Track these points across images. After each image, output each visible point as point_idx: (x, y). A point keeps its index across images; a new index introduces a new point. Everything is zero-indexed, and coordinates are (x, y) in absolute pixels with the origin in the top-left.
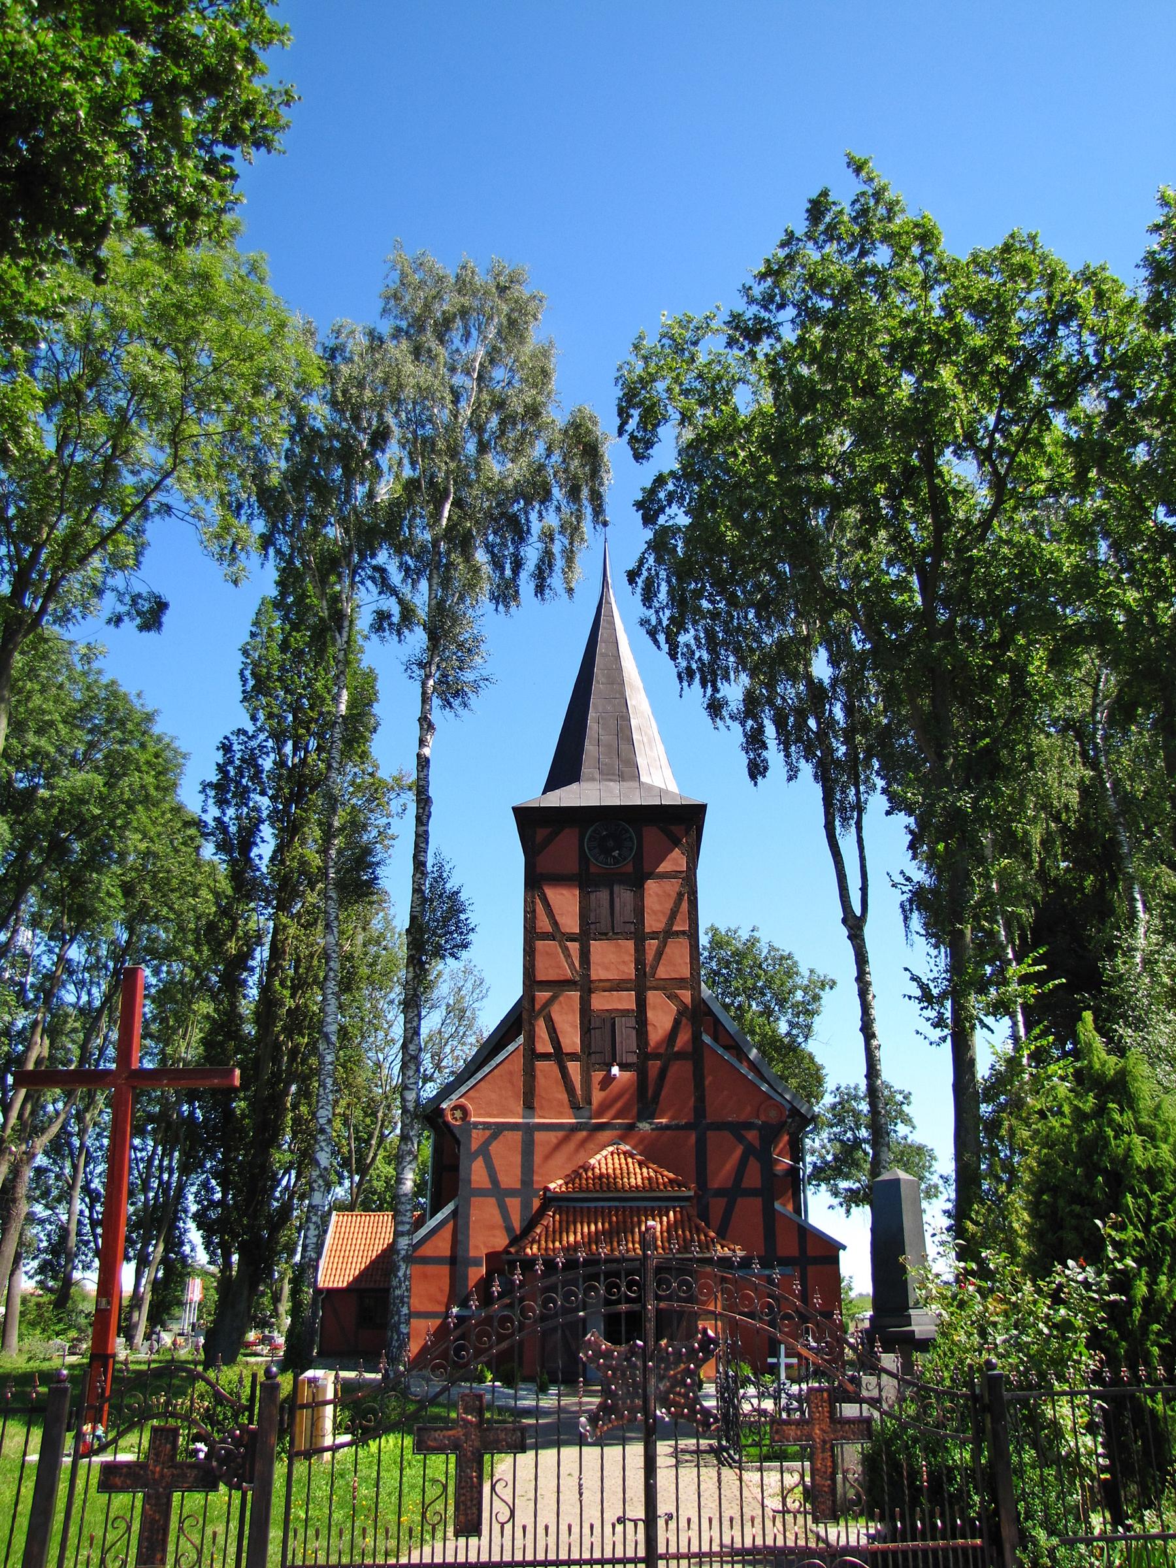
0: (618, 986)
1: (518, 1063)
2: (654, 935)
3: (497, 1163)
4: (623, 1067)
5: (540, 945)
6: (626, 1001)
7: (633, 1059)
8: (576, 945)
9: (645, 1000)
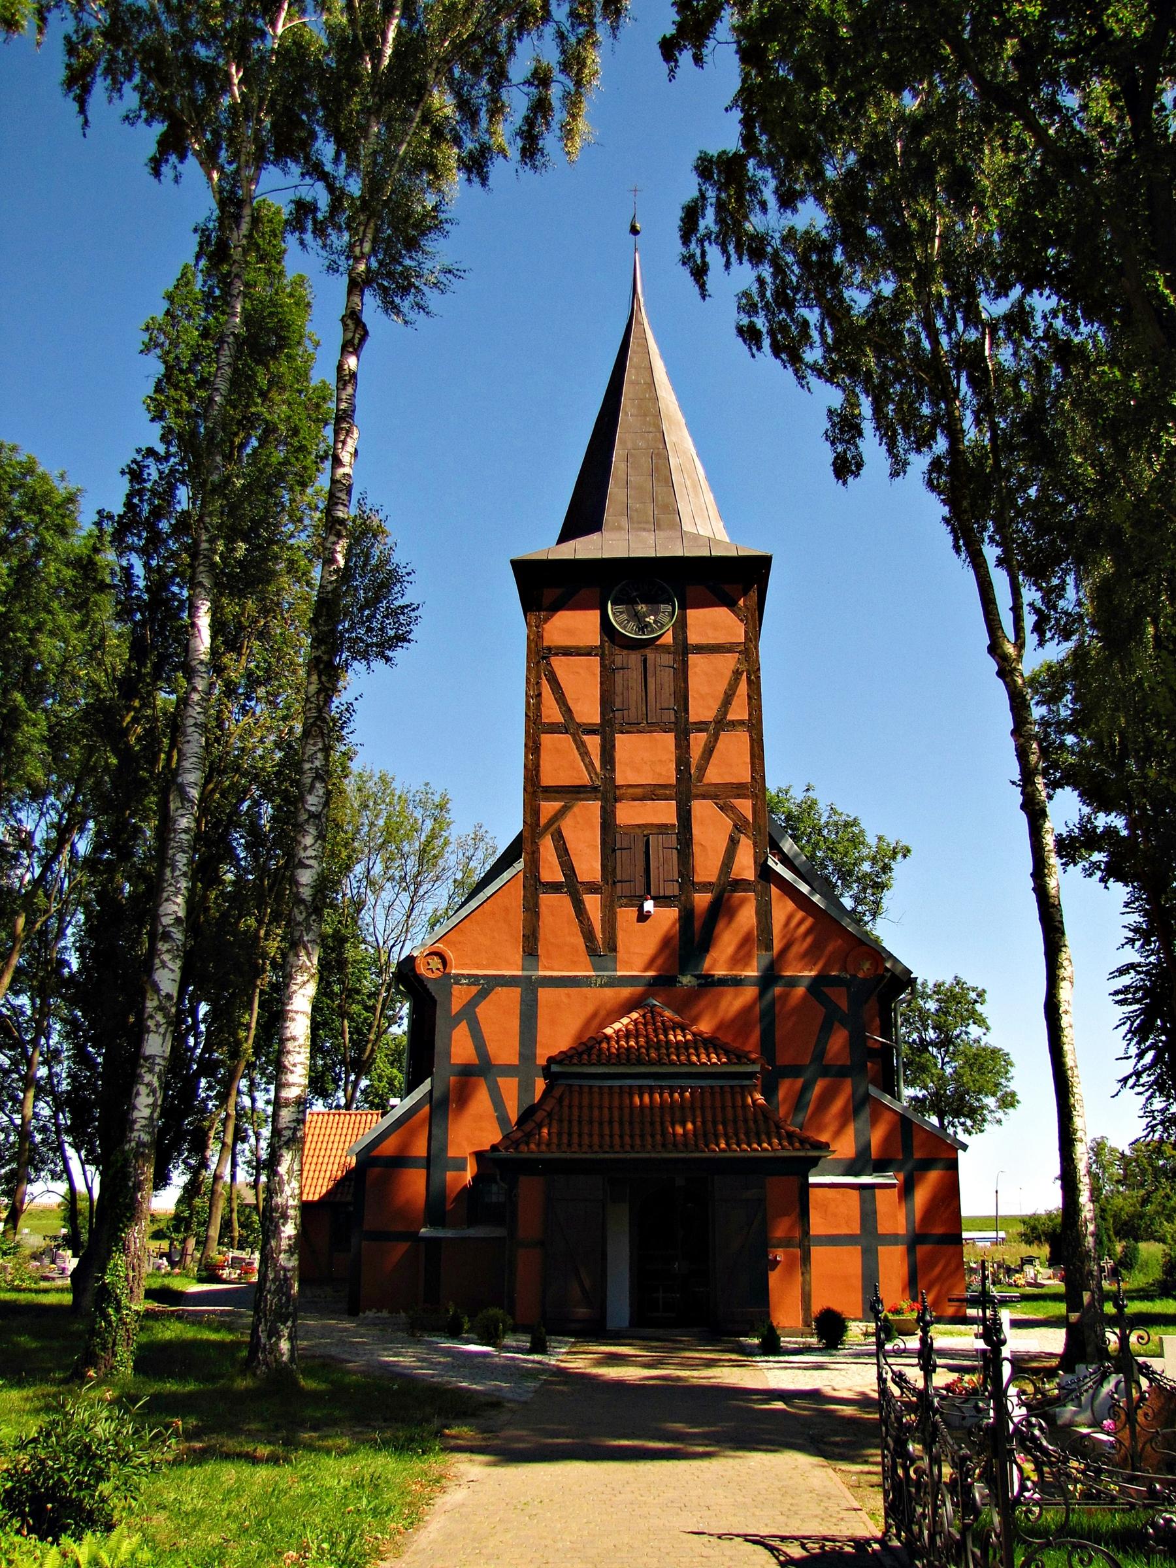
0: (652, 793)
1: (517, 894)
2: (701, 726)
3: (487, 1030)
4: (660, 901)
5: (546, 739)
6: (665, 812)
7: (673, 890)
8: (597, 739)
9: (689, 812)
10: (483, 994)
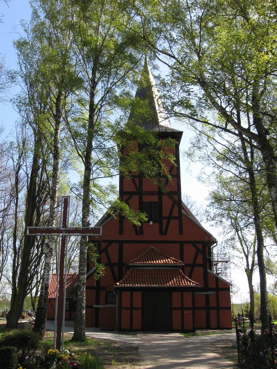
0: (151, 193)
10: (108, 246)
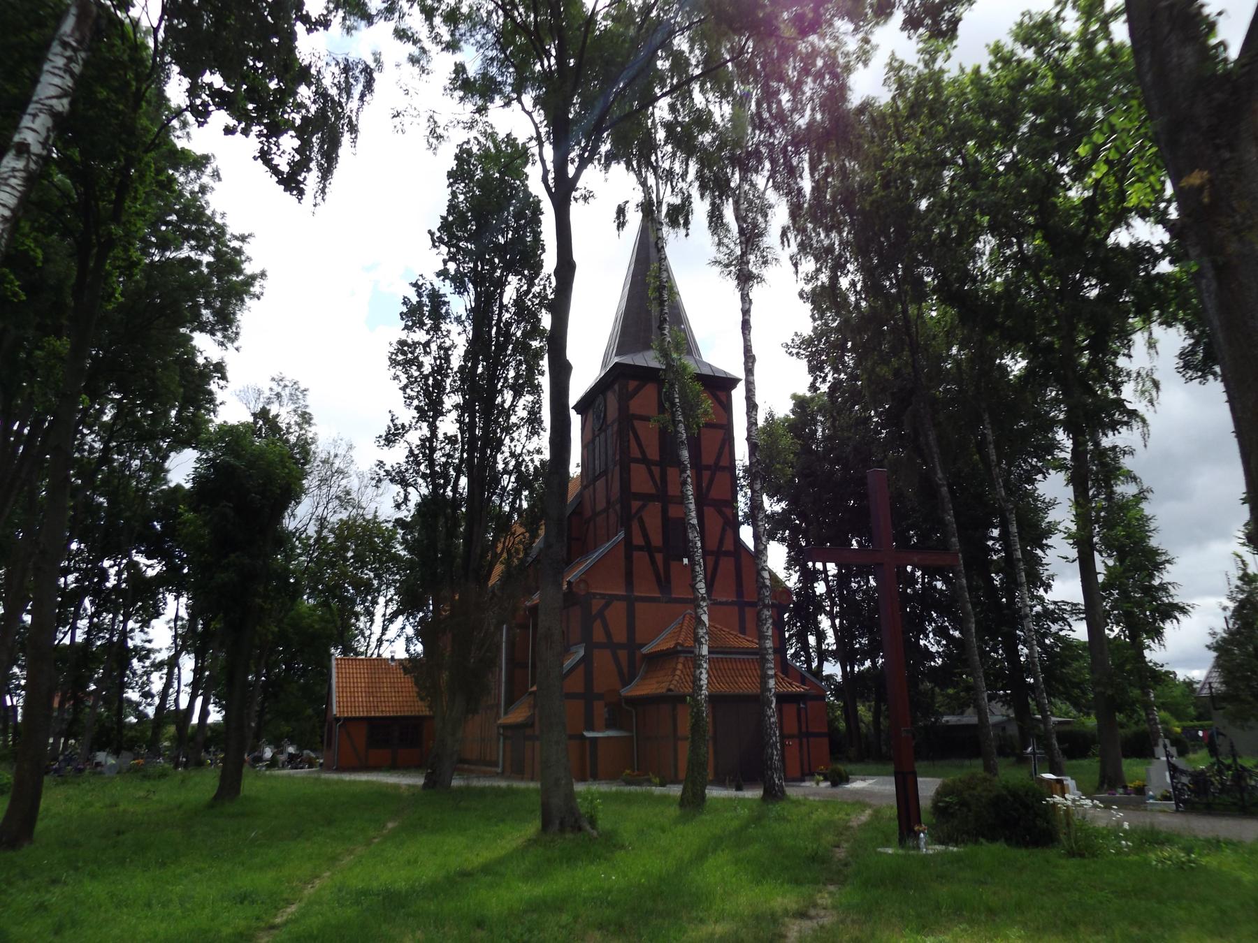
10: (607, 605)
